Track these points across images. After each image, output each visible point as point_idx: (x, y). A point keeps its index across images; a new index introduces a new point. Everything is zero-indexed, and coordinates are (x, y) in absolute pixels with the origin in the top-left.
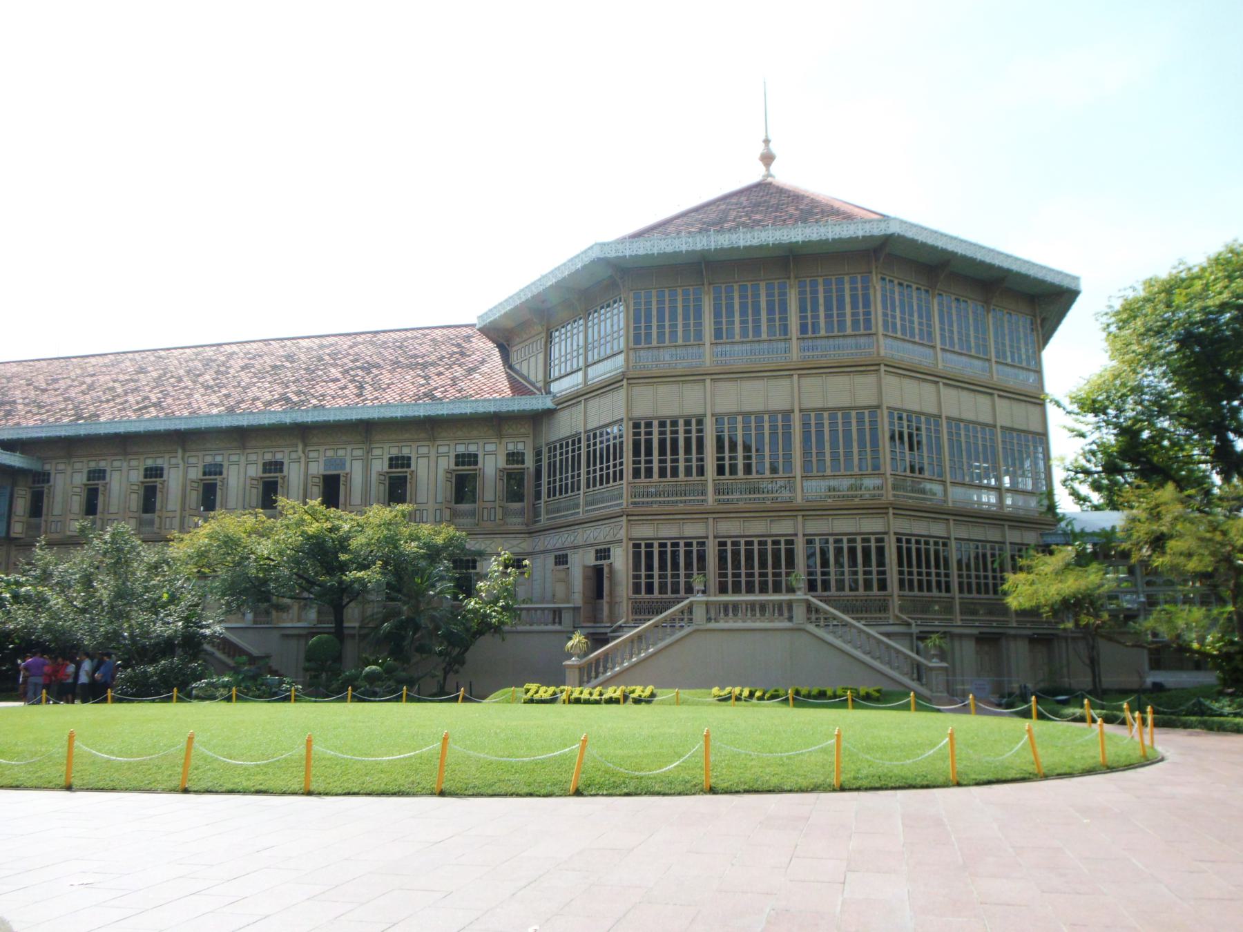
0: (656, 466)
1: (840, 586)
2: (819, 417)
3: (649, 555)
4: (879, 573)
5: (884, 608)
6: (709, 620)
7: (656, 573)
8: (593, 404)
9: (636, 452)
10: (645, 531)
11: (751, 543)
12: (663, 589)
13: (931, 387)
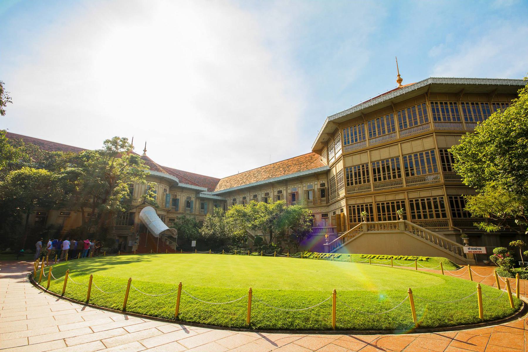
1: (425, 216)
3: (354, 210)
5: (446, 224)
6: (368, 230)
10: (352, 202)
11: (389, 203)
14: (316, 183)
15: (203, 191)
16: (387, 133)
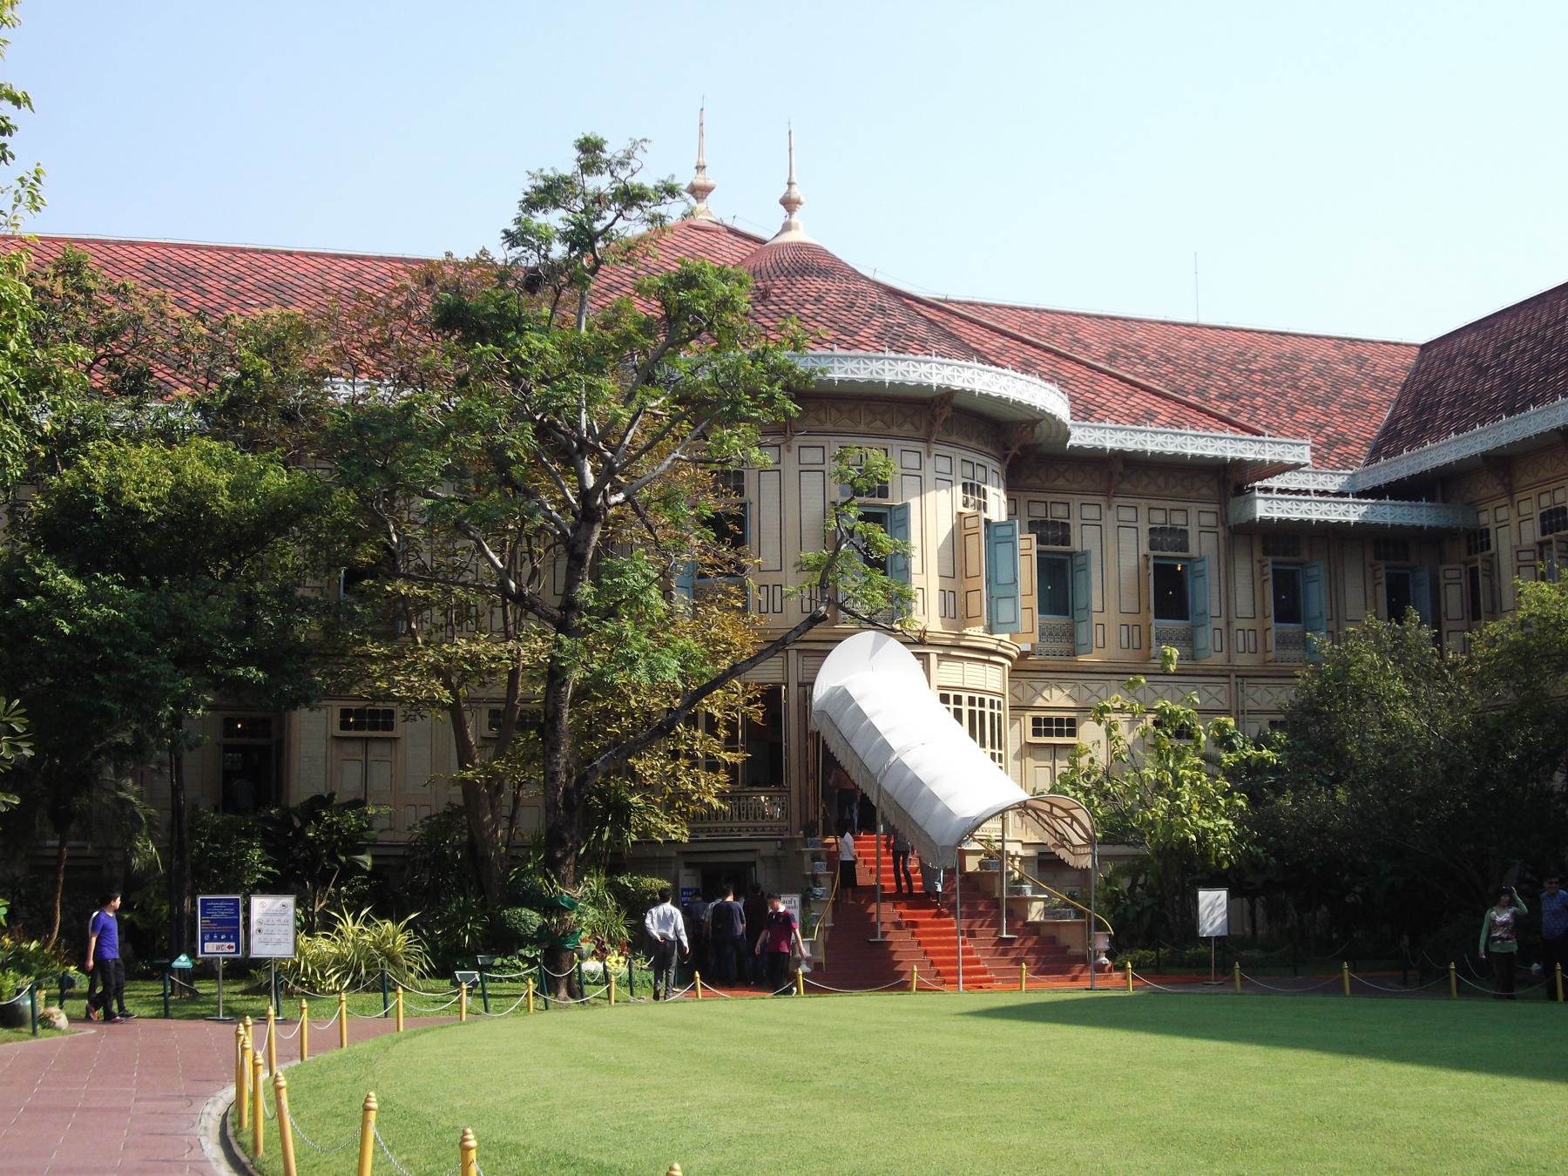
15: (1280, 468)
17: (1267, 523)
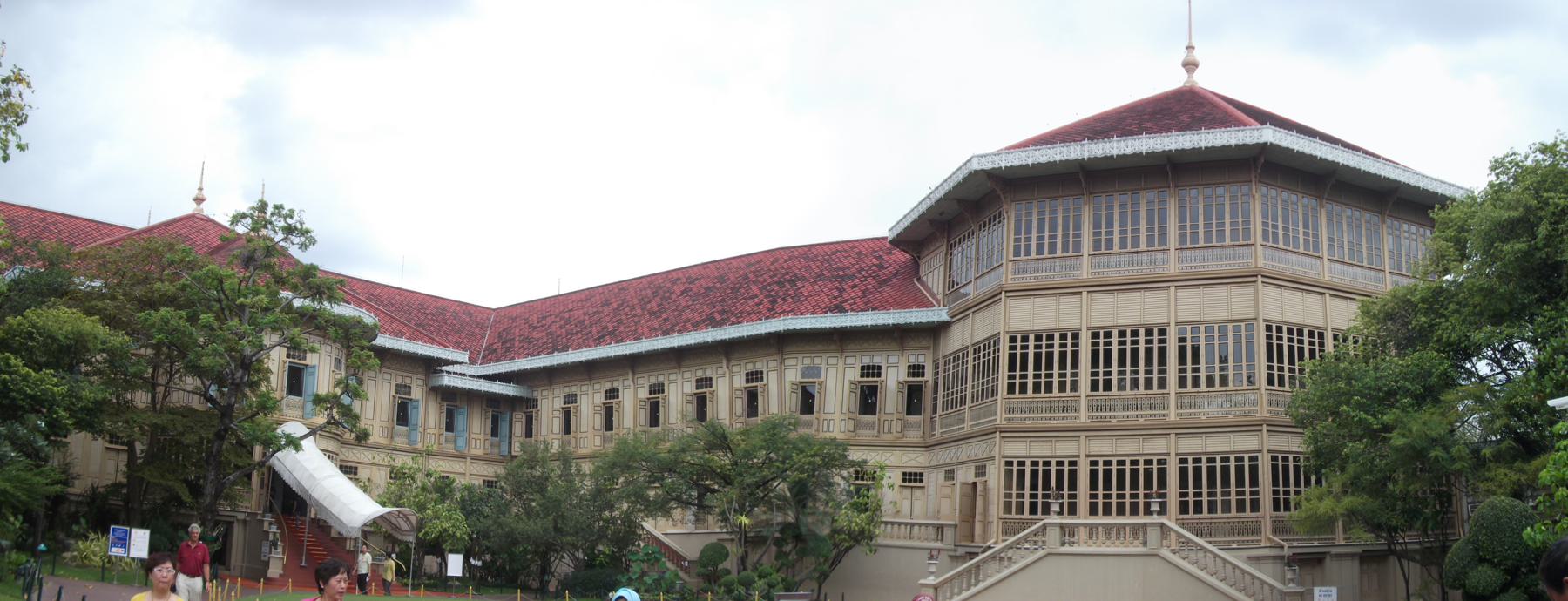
0: (1030, 381)
2: (1195, 331)
3: (1021, 473)
4: (1252, 493)
6: (1063, 544)
7: (1027, 492)
8: (979, 316)
9: (1012, 367)
12: (1033, 510)
13: (1319, 297)
14: (893, 359)
15: (454, 363)
16: (1143, 247)
17: (448, 387)
